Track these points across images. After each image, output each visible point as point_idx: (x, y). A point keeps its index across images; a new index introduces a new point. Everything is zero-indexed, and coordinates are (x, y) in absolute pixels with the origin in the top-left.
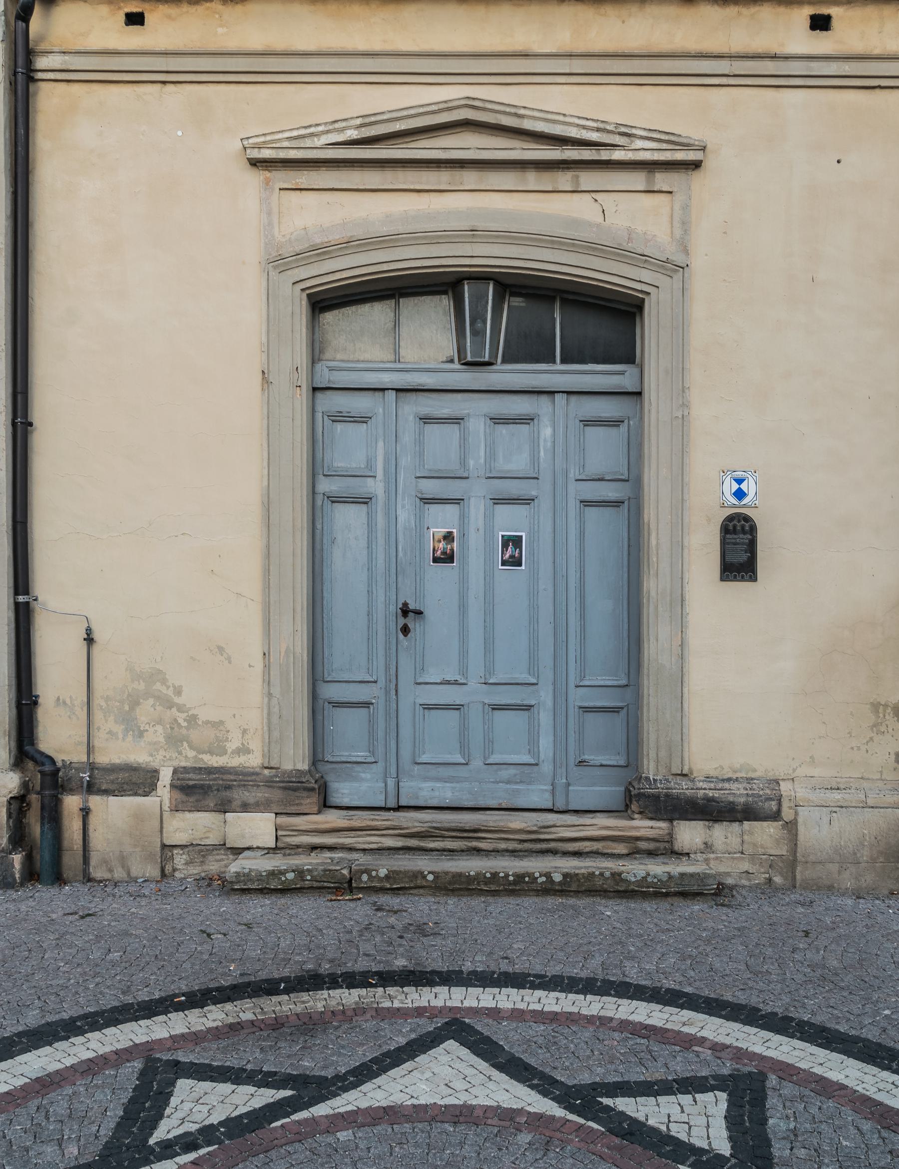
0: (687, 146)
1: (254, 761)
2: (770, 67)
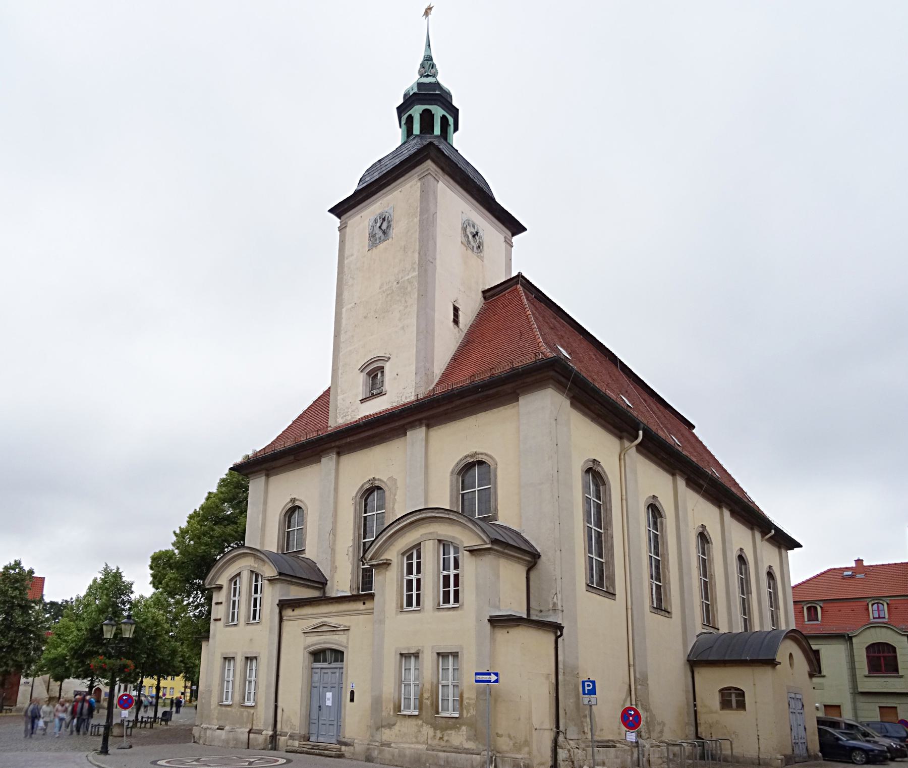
0: (346, 627)
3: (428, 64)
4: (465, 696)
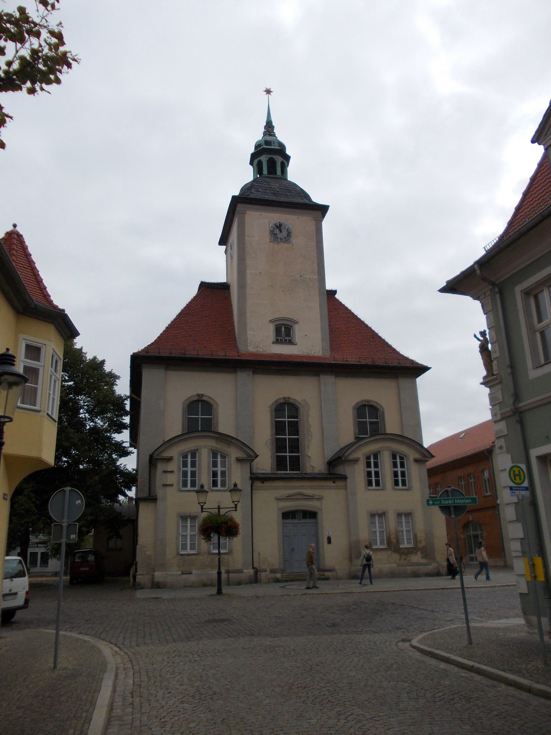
3: (269, 127)
4: (419, 535)
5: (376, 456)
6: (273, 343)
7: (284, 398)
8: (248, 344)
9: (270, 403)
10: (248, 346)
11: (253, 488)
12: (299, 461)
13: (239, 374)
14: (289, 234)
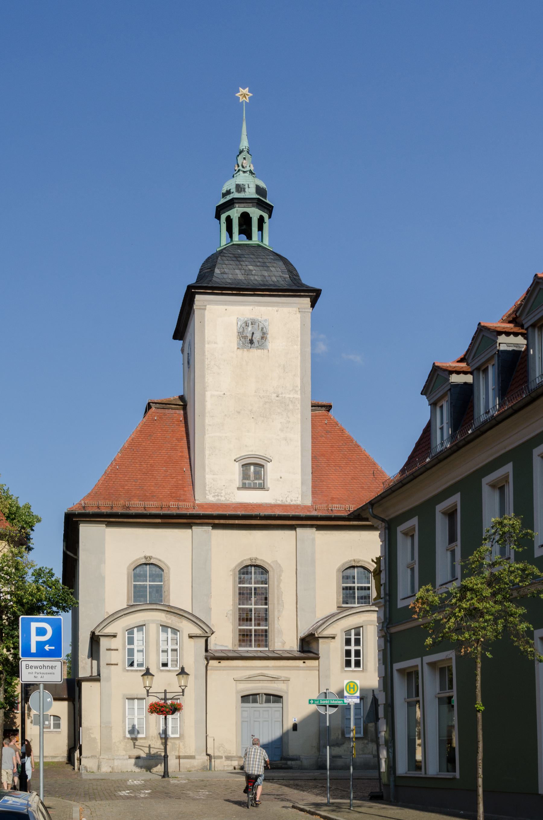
0: (288, 678)
1: (235, 755)
2: (298, 668)
5: (357, 634)
6: (239, 488)
7: (251, 560)
8: (207, 492)
9: (233, 566)
10: (206, 494)
11: (208, 668)
12: (266, 636)
13: (194, 528)
14: (264, 337)
